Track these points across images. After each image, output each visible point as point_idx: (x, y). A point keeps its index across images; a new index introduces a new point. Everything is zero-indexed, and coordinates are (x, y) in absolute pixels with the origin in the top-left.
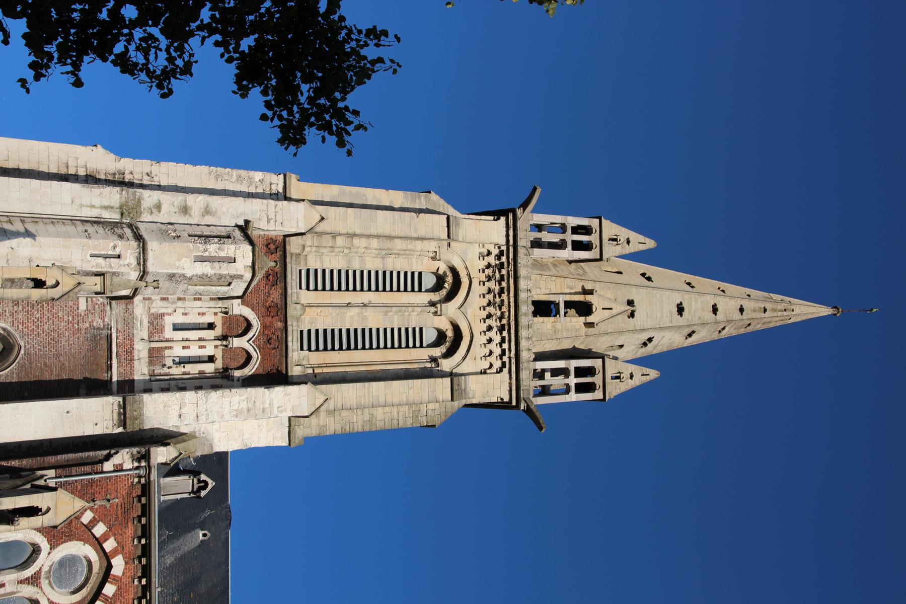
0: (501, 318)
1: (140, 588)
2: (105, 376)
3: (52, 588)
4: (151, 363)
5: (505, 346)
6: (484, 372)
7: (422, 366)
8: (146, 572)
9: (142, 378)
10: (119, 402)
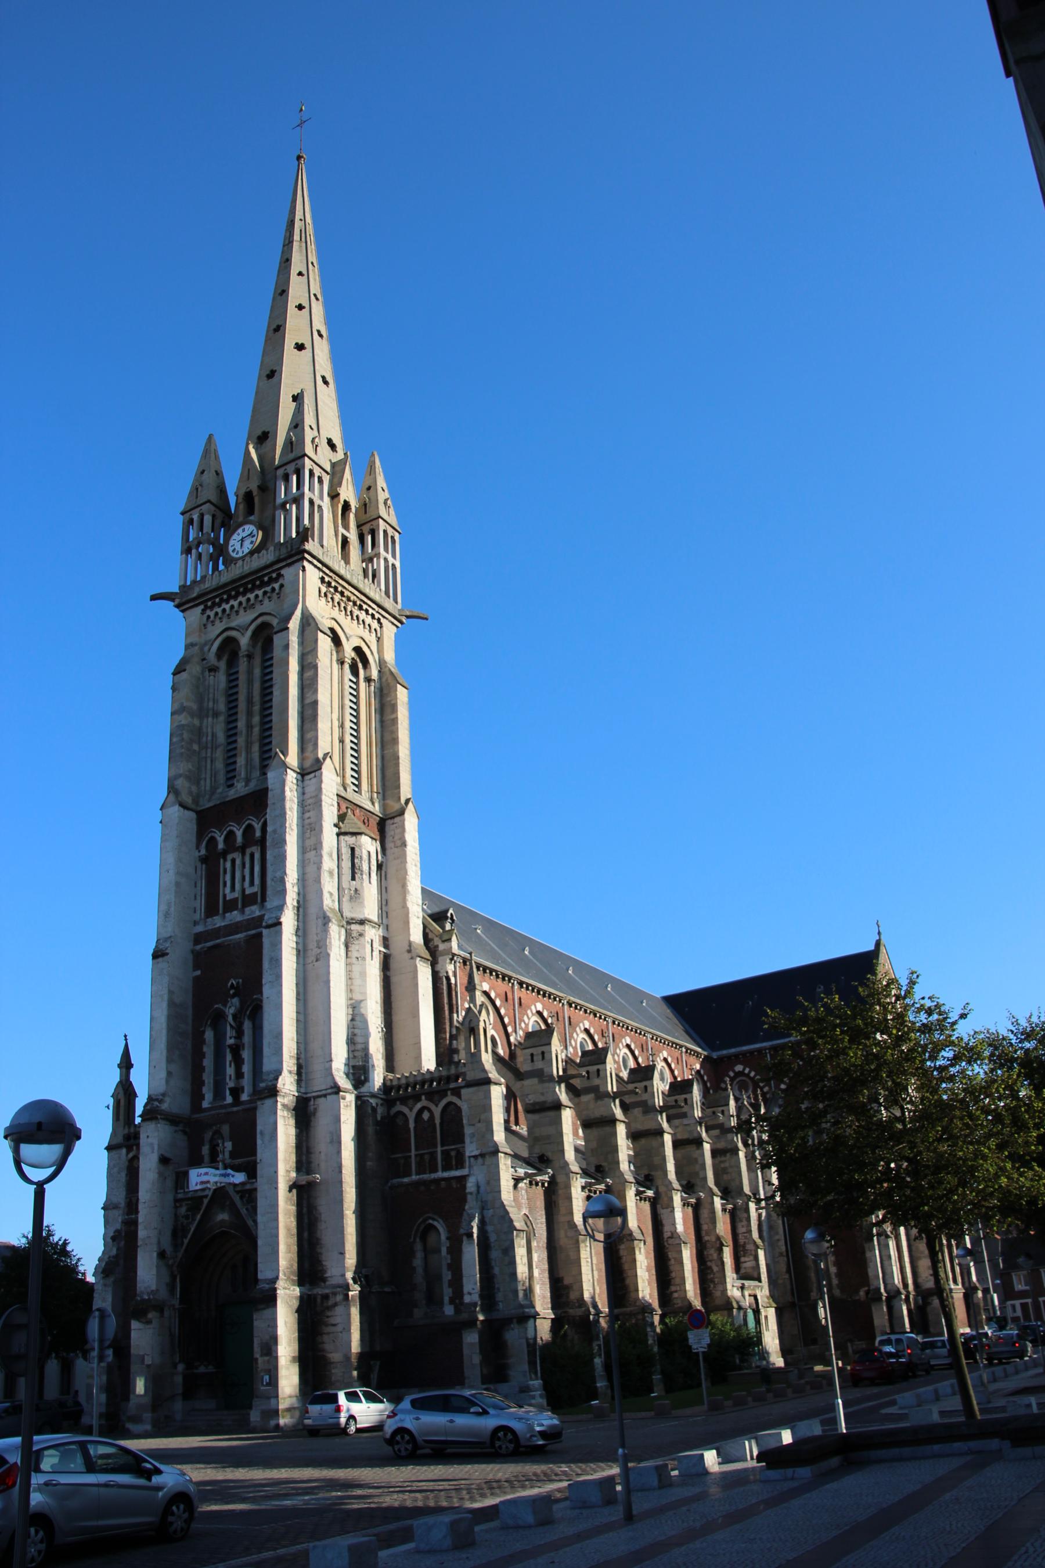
0: (355, 603)
5: (371, 611)
6: (379, 639)
7: (373, 695)
8: (491, 971)
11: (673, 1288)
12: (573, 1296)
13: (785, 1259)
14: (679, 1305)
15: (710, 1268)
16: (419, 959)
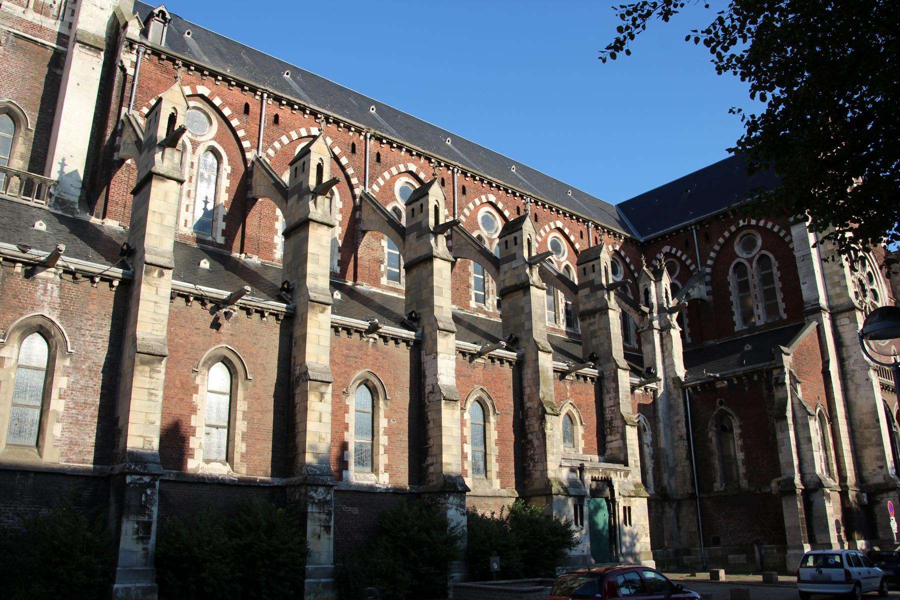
1: (223, 82)
2: (50, 53)
3: (204, 135)
4: (47, 15)
8: (214, 74)
9: (59, 26)
10: (80, 46)
11: (430, 460)
12: (121, 446)
13: (686, 443)
14: (434, 483)
15: (530, 442)
16: (77, 45)
